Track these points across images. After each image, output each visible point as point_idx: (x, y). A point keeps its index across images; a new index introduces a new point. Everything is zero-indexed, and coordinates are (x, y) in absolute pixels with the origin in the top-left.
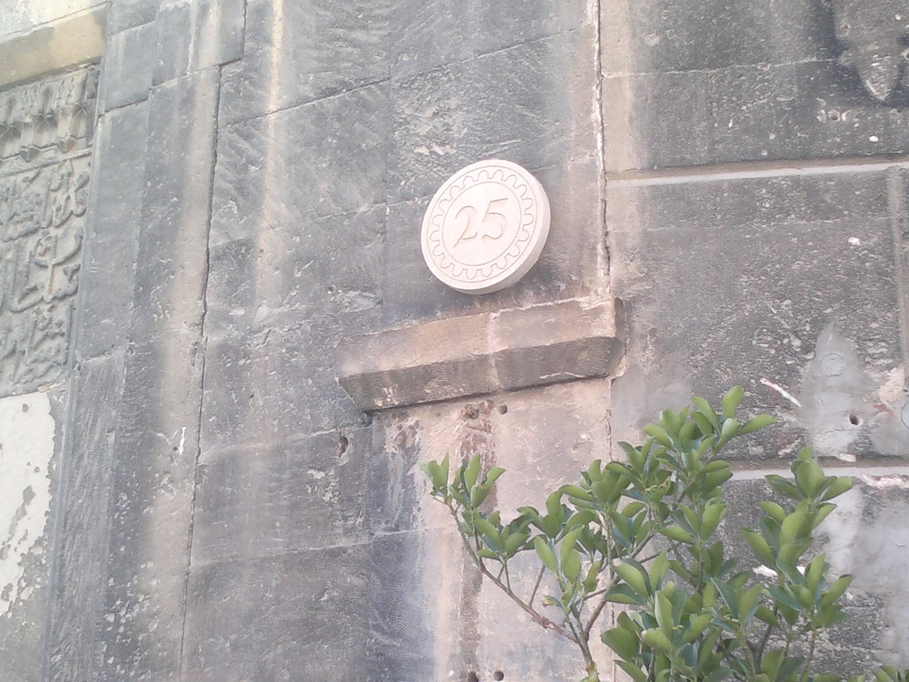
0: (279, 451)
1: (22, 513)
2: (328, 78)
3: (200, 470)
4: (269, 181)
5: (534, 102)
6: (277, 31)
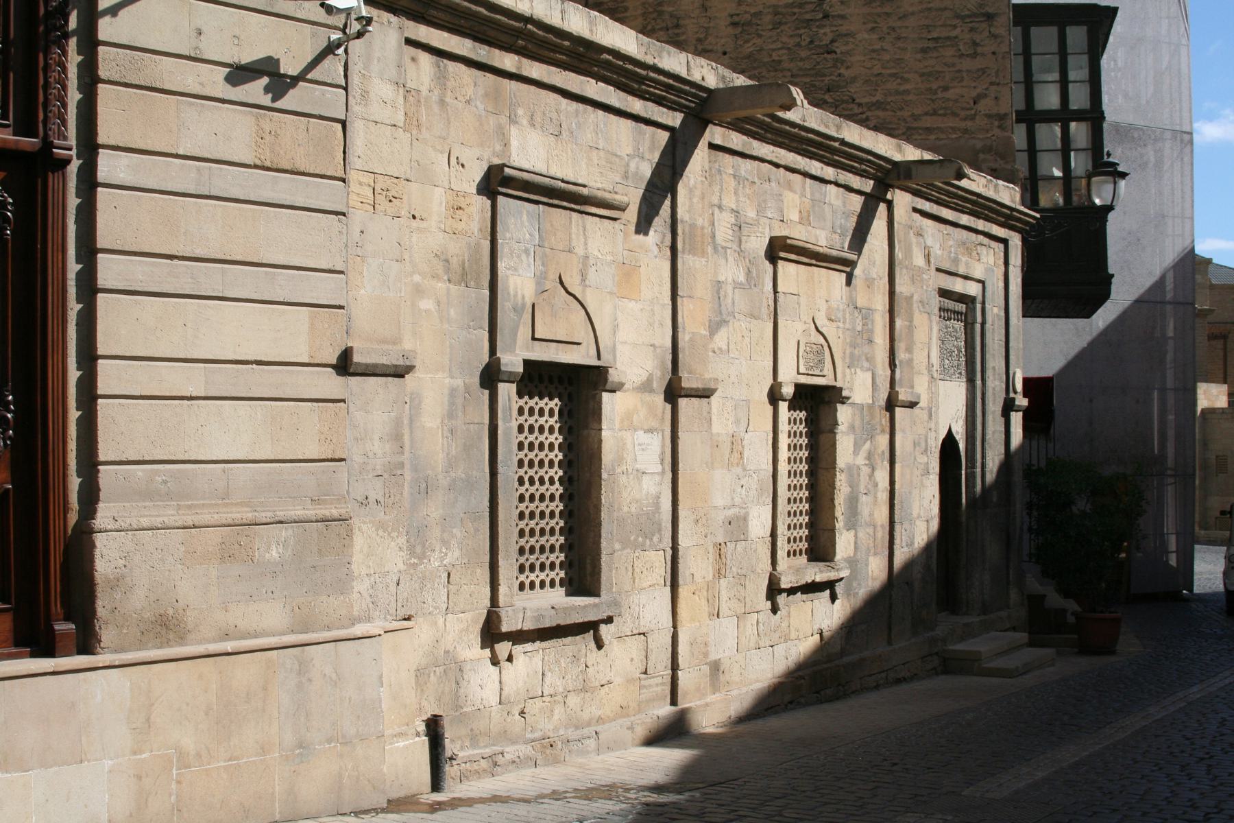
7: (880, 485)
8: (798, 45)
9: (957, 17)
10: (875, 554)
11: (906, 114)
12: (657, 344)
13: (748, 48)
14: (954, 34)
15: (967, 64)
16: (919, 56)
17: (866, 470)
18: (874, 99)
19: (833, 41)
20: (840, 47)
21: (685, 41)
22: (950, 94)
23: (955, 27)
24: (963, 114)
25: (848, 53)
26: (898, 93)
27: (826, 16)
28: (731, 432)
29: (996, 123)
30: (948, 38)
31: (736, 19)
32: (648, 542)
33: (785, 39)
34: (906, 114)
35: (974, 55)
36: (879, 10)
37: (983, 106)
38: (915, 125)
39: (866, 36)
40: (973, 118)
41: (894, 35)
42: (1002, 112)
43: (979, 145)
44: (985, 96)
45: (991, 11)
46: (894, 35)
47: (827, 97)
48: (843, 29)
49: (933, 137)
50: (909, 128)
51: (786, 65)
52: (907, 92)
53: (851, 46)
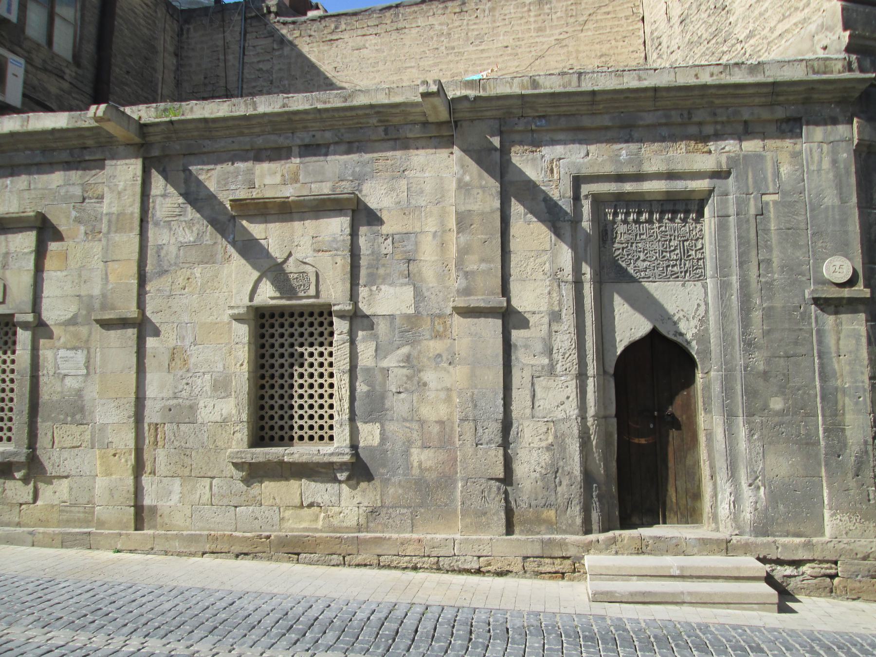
0: (784, 307)
1: (697, 310)
2: (788, 226)
3: (764, 309)
4: (774, 246)
5: (847, 245)
6: (772, 210)
7: (432, 385)
10: (425, 447)
12: (83, 294)
17: (397, 376)
28: (171, 346)
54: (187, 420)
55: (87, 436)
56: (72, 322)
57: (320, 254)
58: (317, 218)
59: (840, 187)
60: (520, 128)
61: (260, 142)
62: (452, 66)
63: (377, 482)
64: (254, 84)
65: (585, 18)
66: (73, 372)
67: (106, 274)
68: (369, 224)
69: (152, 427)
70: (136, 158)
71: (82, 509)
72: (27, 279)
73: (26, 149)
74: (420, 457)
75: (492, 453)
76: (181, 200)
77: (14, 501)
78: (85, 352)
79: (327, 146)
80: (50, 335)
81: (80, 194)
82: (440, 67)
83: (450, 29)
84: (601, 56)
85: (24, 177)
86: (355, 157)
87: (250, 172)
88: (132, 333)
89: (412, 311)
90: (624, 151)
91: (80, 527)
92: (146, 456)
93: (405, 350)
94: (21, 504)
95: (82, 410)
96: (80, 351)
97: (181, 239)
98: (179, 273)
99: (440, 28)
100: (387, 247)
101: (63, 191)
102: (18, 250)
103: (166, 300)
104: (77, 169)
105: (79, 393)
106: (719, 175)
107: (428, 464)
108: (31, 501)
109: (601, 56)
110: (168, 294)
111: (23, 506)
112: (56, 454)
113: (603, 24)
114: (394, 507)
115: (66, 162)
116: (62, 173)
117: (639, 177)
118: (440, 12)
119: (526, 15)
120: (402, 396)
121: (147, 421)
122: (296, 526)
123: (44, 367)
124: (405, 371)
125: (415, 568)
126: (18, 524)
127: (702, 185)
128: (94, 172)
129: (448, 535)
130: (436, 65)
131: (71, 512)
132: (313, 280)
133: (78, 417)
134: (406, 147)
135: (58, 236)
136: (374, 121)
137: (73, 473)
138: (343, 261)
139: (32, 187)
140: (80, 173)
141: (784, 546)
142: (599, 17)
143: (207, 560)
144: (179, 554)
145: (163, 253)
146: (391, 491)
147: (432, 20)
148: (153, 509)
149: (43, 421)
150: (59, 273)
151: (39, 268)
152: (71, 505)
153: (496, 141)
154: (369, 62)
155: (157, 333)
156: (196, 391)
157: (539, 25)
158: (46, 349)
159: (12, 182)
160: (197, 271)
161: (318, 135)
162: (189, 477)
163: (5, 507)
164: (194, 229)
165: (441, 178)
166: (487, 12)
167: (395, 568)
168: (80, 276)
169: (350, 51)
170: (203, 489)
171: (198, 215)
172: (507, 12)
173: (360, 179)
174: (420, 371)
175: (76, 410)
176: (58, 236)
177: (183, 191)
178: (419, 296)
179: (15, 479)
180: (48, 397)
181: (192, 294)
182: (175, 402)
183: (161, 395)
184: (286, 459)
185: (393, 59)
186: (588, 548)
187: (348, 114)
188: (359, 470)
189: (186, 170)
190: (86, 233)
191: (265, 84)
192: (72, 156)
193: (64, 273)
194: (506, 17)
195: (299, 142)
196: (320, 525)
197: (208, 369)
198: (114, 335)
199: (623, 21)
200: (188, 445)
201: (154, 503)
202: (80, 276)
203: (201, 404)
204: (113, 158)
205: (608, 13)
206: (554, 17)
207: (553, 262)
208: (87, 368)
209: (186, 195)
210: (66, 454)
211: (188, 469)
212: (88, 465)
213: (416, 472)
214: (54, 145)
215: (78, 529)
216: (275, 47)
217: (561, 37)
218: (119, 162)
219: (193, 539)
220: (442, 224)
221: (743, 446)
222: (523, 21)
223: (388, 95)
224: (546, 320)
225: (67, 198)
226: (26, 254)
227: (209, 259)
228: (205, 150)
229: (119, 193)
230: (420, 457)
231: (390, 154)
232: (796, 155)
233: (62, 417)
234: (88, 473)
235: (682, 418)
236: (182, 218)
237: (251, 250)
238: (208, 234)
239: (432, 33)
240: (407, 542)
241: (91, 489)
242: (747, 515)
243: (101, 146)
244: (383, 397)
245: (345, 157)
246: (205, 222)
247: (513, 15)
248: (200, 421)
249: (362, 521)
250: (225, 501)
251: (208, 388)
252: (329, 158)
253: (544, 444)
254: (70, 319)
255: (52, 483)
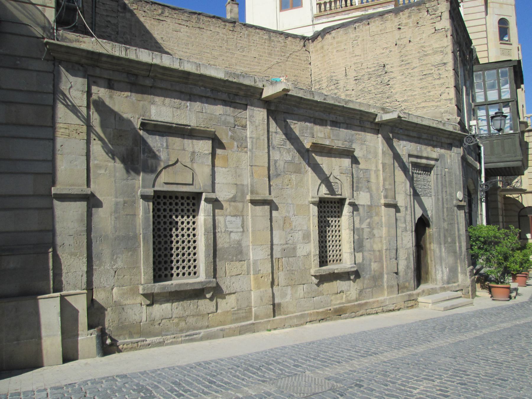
7: (376, 235)
8: (377, 84)
9: (432, 66)
11: (415, 103)
12: (238, 183)
13: (360, 87)
14: (431, 72)
15: (437, 82)
16: (419, 82)
17: (367, 230)
18: (404, 99)
19: (389, 81)
20: (391, 83)
21: (340, 88)
22: (431, 94)
23: (432, 69)
24: (436, 100)
25: (394, 84)
26: (412, 96)
27: (386, 73)
28: (284, 216)
29: (449, 102)
30: (430, 74)
31: (356, 78)
32: (235, 258)
33: (372, 83)
34: (415, 103)
35: (439, 79)
36: (404, 68)
37: (444, 96)
38: (419, 106)
39: (400, 77)
40: (440, 101)
41: (410, 75)
42: (451, 98)
43: (442, 110)
44: (444, 93)
45: (445, 61)
46: (410, 75)
47: (387, 101)
48: (391, 77)
49: (425, 110)
50: (416, 108)
51: (373, 91)
52: (415, 95)
53: (395, 82)
54: (292, 256)
55: (245, 267)
56: (233, 200)
57: (342, 175)
58: (340, 158)
59: (459, 169)
60: (396, 131)
61: (317, 114)
62: (229, 59)
63: (361, 279)
64: (104, 30)
65: (288, 55)
66: (235, 230)
67: (252, 173)
68: (356, 164)
69: (277, 260)
70: (264, 108)
71: (244, 311)
72: (208, 170)
73: (202, 86)
74: (374, 266)
75: (394, 262)
76: (284, 137)
77: (205, 313)
78: (241, 218)
79: (340, 123)
80: (221, 207)
81: (233, 122)
82: (223, 58)
83: (228, 38)
84: (295, 76)
85: (198, 104)
86: (349, 131)
87: (312, 129)
88: (267, 208)
89: (369, 204)
90: (419, 146)
91: (244, 321)
92: (275, 276)
93: (368, 220)
94: (209, 314)
95: (241, 252)
96: (238, 217)
97: (285, 158)
98: (285, 176)
99: (222, 35)
100: (361, 176)
101: (223, 118)
102: (201, 151)
103: (280, 191)
104: (230, 106)
105: (239, 243)
106: (437, 160)
107: (376, 269)
108: (215, 311)
109: (295, 76)
110: (281, 187)
111: (210, 315)
112: (228, 280)
113: (295, 61)
114: (367, 288)
115: (224, 100)
116: (222, 106)
117: (421, 157)
118: (222, 26)
119: (263, 44)
120: (368, 240)
121: (274, 257)
122: (336, 303)
123: (219, 227)
124: (369, 230)
125: (377, 313)
126: (208, 327)
127: (432, 163)
128: (240, 111)
129: (385, 297)
130: (221, 55)
131: (238, 313)
132: (340, 186)
133: (239, 257)
134: (365, 131)
135: (222, 146)
136: (358, 117)
137: (238, 290)
138: (349, 179)
139: (204, 111)
140: (232, 109)
141: (455, 287)
142: (294, 57)
143: (309, 326)
144: (297, 326)
145: (277, 165)
146: (366, 282)
147: (218, 29)
148: (279, 305)
149: (220, 261)
150: (224, 169)
151: (213, 165)
152: (238, 310)
153: (391, 135)
154: (183, 41)
155: (277, 209)
156: (296, 240)
157: (269, 51)
158: (219, 216)
159: (190, 105)
160: (293, 177)
161: (338, 117)
162: (293, 285)
163: (199, 317)
164: (291, 154)
165: (376, 148)
166: (246, 35)
167: (372, 314)
168: (236, 173)
169: (171, 31)
170: (301, 291)
171: (292, 147)
172: (255, 39)
173: (351, 141)
174: (373, 229)
175: (239, 253)
176: (222, 146)
177: (285, 132)
178: (371, 196)
179: (205, 298)
180: (222, 246)
181: (292, 188)
182: (286, 246)
183: (280, 243)
184: (336, 271)
185: (197, 44)
186: (418, 295)
187: (352, 112)
188: (357, 274)
189: (285, 121)
190: (238, 147)
191: (113, 33)
192: (229, 98)
193: (227, 169)
194: (255, 42)
195: (331, 119)
196: (344, 300)
197: (300, 229)
198: (259, 208)
199: (303, 62)
200: (293, 269)
201: (279, 302)
202: (236, 173)
203: (298, 247)
204: (252, 106)
205: (297, 56)
206: (276, 50)
207: (405, 187)
208: (243, 227)
209: (286, 134)
210: (233, 279)
211: (294, 281)
212: (245, 284)
213: (373, 272)
214: (221, 89)
215: (244, 322)
216: (120, 9)
217: (279, 61)
218: (255, 108)
219: (302, 316)
220: (376, 167)
221: (443, 254)
222: (262, 47)
223: (359, 105)
224: (404, 209)
225: (226, 123)
226: (206, 154)
227: (298, 171)
228: (295, 113)
229: (256, 127)
230: (374, 266)
231: (360, 133)
232: (451, 156)
233: (230, 257)
234: (246, 289)
235: (423, 246)
236: (284, 147)
237: (317, 169)
238: (297, 157)
239: (218, 37)
240: (374, 302)
241: (249, 299)
242: (445, 278)
243: (246, 96)
244: (362, 241)
245: (346, 130)
246: (295, 151)
247: (258, 42)
248: (298, 255)
249: (357, 296)
250: (310, 295)
251: (300, 239)
252: (341, 129)
253: (405, 258)
254: (232, 198)
255: (225, 298)
